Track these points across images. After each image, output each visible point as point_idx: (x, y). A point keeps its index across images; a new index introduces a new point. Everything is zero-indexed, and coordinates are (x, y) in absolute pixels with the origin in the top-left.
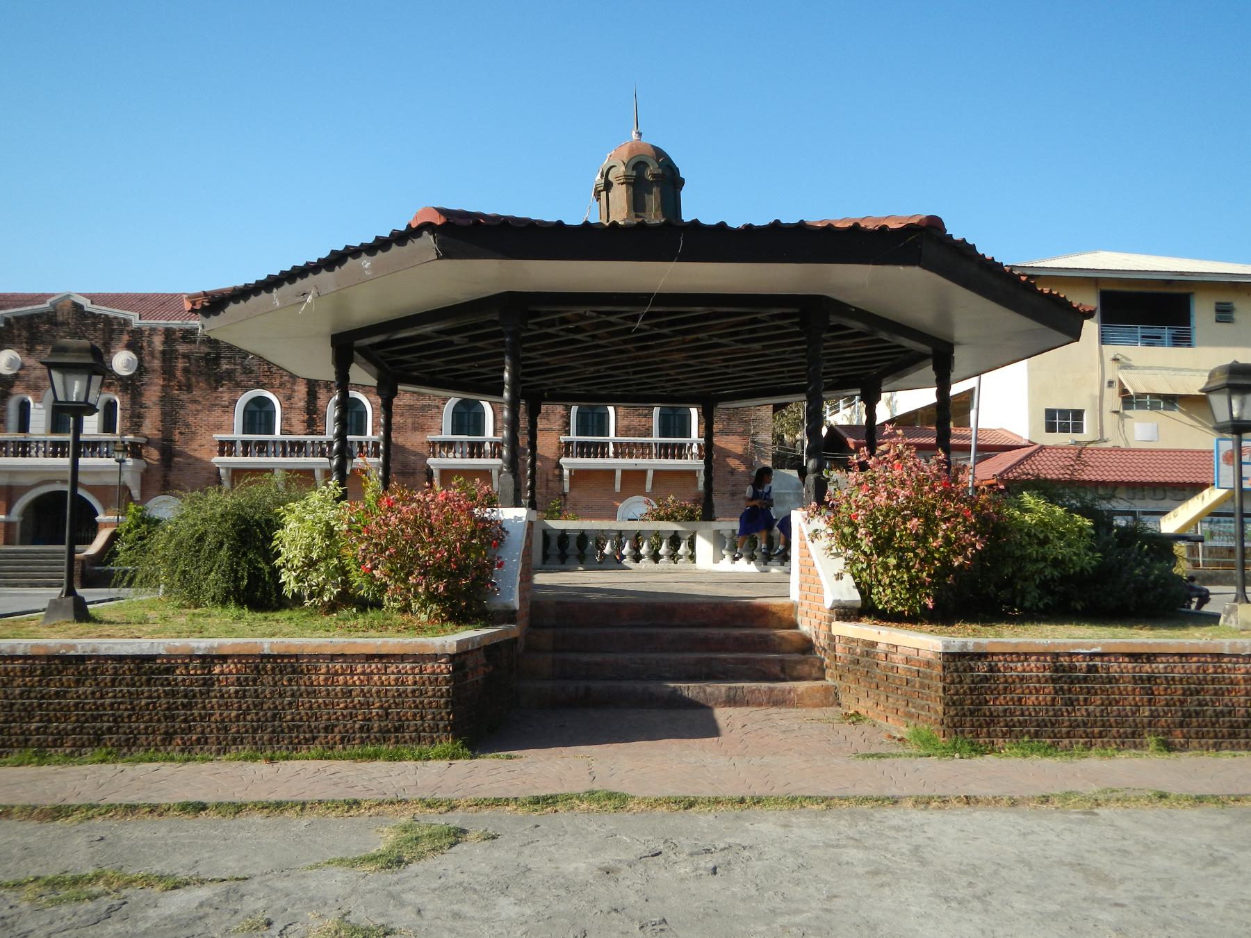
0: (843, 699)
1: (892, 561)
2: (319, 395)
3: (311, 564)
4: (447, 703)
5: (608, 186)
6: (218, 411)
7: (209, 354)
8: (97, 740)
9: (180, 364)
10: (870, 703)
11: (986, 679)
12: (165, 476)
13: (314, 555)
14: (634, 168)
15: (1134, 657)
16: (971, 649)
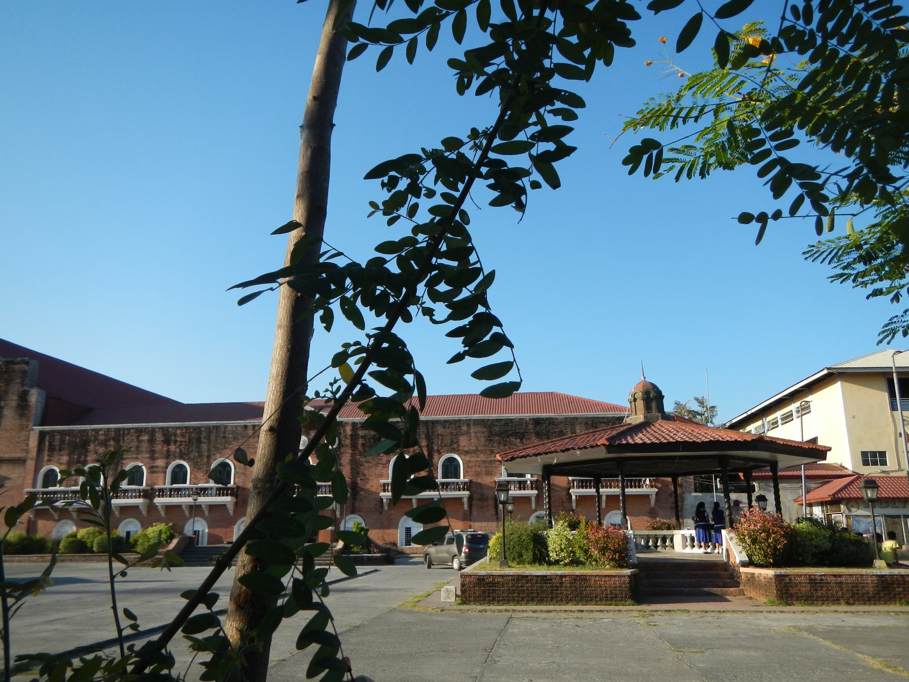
0: (746, 593)
1: (758, 547)
2: (434, 457)
3: (562, 550)
4: (629, 590)
5: (635, 400)
6: (380, 467)
7: (375, 435)
8: (533, 600)
9: (360, 441)
10: (754, 593)
11: (789, 583)
12: (353, 504)
13: (563, 546)
14: (645, 394)
15: (835, 576)
16: (783, 573)
